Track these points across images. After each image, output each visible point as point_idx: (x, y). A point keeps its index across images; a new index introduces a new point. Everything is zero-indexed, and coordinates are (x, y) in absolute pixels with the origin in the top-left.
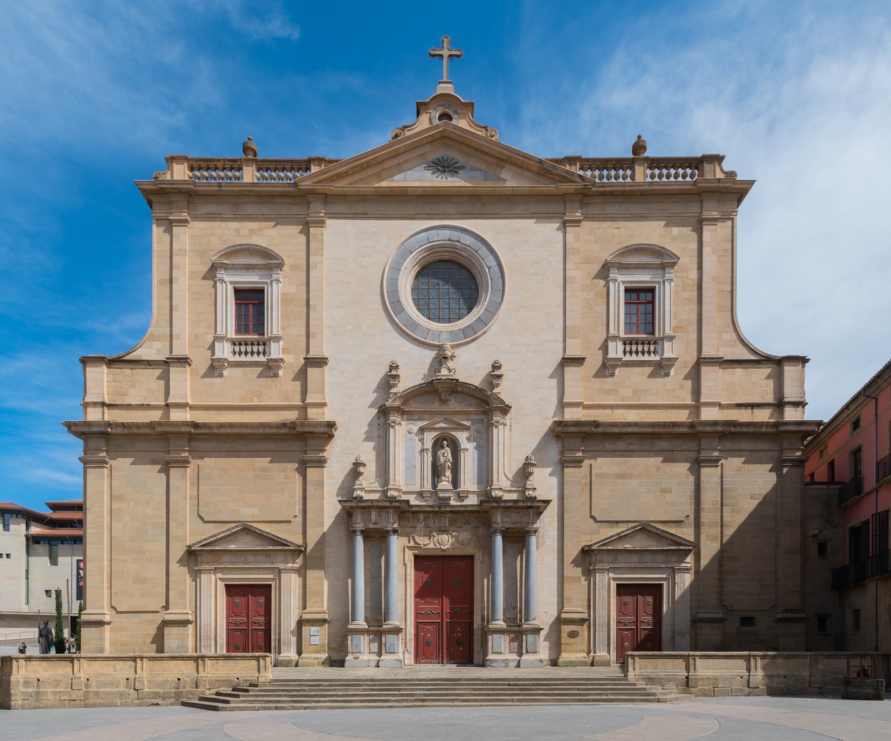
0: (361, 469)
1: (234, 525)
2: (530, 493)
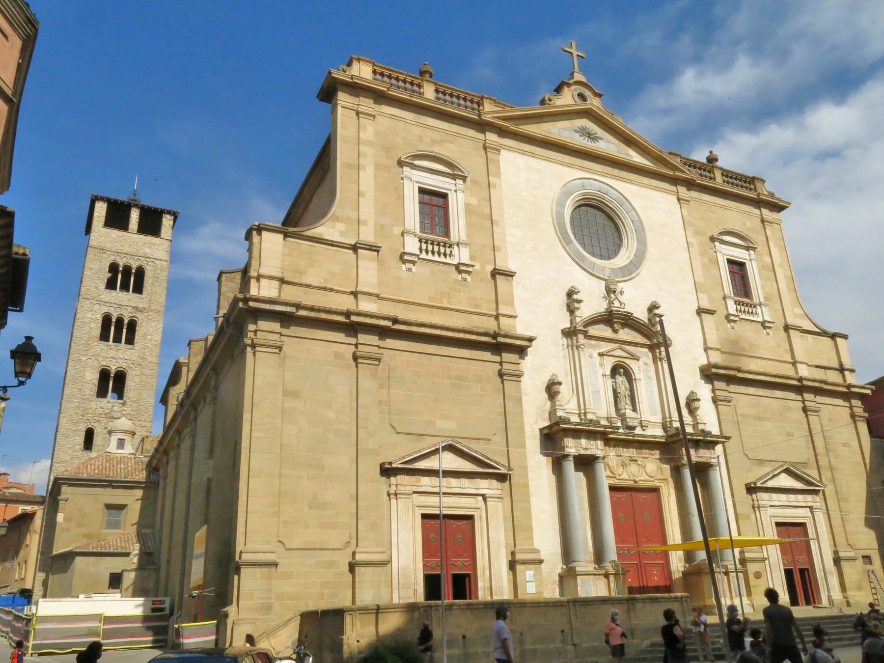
0: (556, 388)
1: (443, 439)
2: (701, 427)
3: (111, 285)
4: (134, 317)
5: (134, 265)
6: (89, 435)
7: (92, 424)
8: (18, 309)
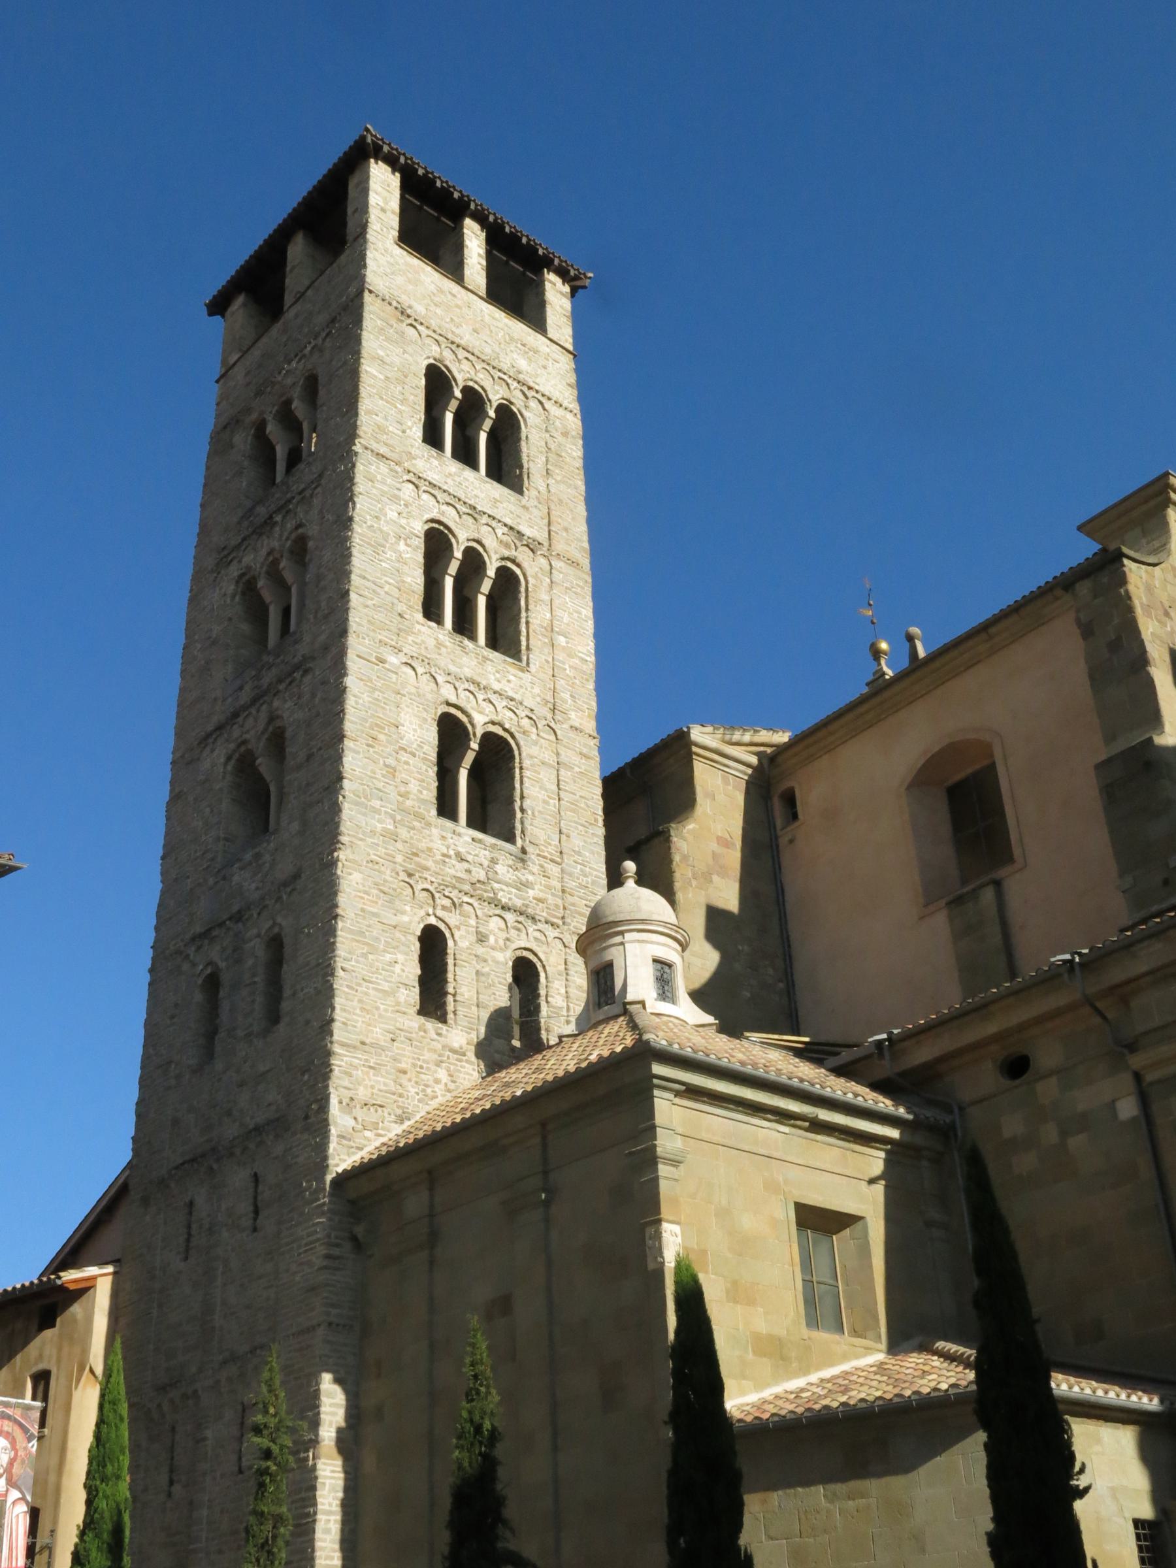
5: (495, 395)
7: (440, 913)
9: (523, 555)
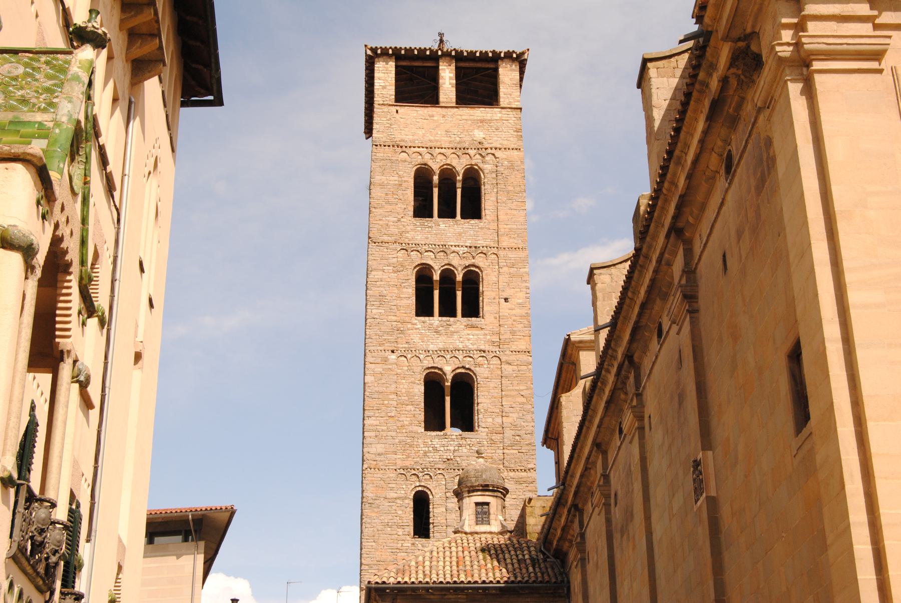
3: (422, 210)
4: (474, 266)
6: (421, 503)
8: (211, 98)
9: (480, 261)
